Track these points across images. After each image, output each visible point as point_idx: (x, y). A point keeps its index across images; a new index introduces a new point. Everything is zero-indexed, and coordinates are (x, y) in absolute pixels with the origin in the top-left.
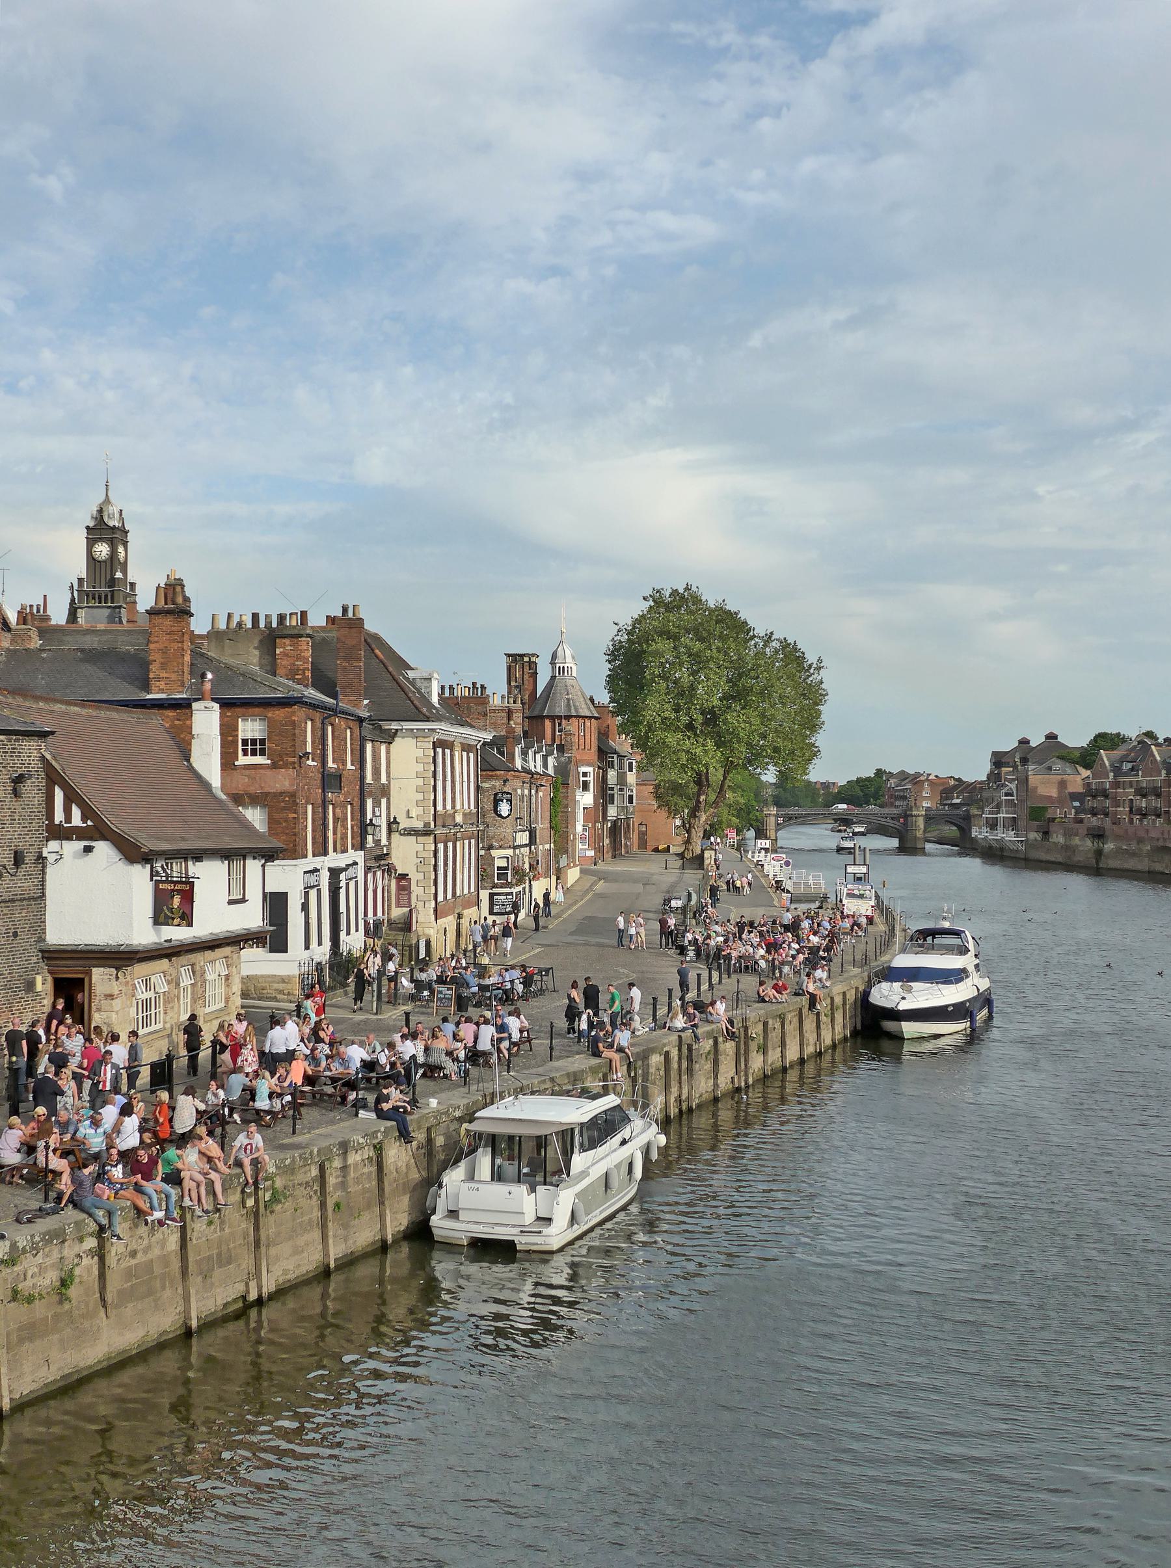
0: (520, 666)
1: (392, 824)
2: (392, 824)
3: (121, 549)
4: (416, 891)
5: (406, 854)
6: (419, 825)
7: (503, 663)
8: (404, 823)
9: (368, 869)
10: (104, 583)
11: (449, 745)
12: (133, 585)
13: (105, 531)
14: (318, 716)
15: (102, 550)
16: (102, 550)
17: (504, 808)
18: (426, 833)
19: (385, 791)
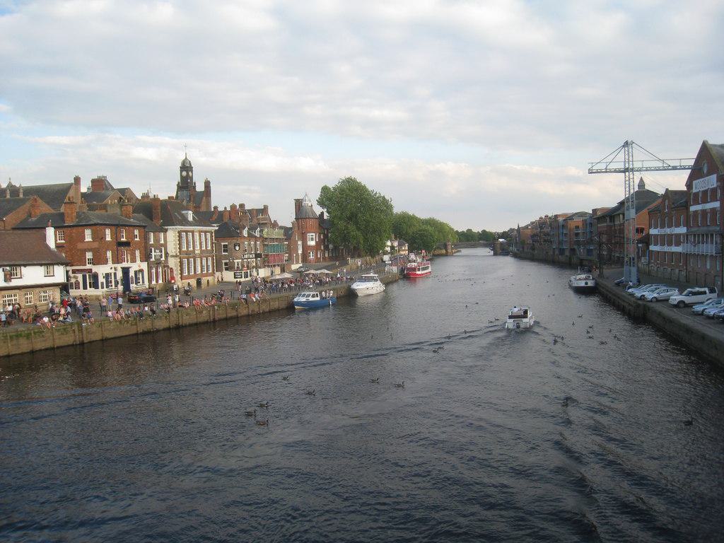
0: (299, 204)
1: (167, 254)
2: (167, 254)
3: (190, 173)
4: (175, 272)
5: (173, 263)
6: (174, 254)
7: (294, 202)
8: (170, 254)
9: (150, 268)
10: (186, 183)
11: (193, 232)
12: (195, 183)
13: (186, 167)
14: (113, 228)
15: (184, 173)
16: (184, 173)
17: (237, 248)
18: (176, 256)
19: (165, 245)
